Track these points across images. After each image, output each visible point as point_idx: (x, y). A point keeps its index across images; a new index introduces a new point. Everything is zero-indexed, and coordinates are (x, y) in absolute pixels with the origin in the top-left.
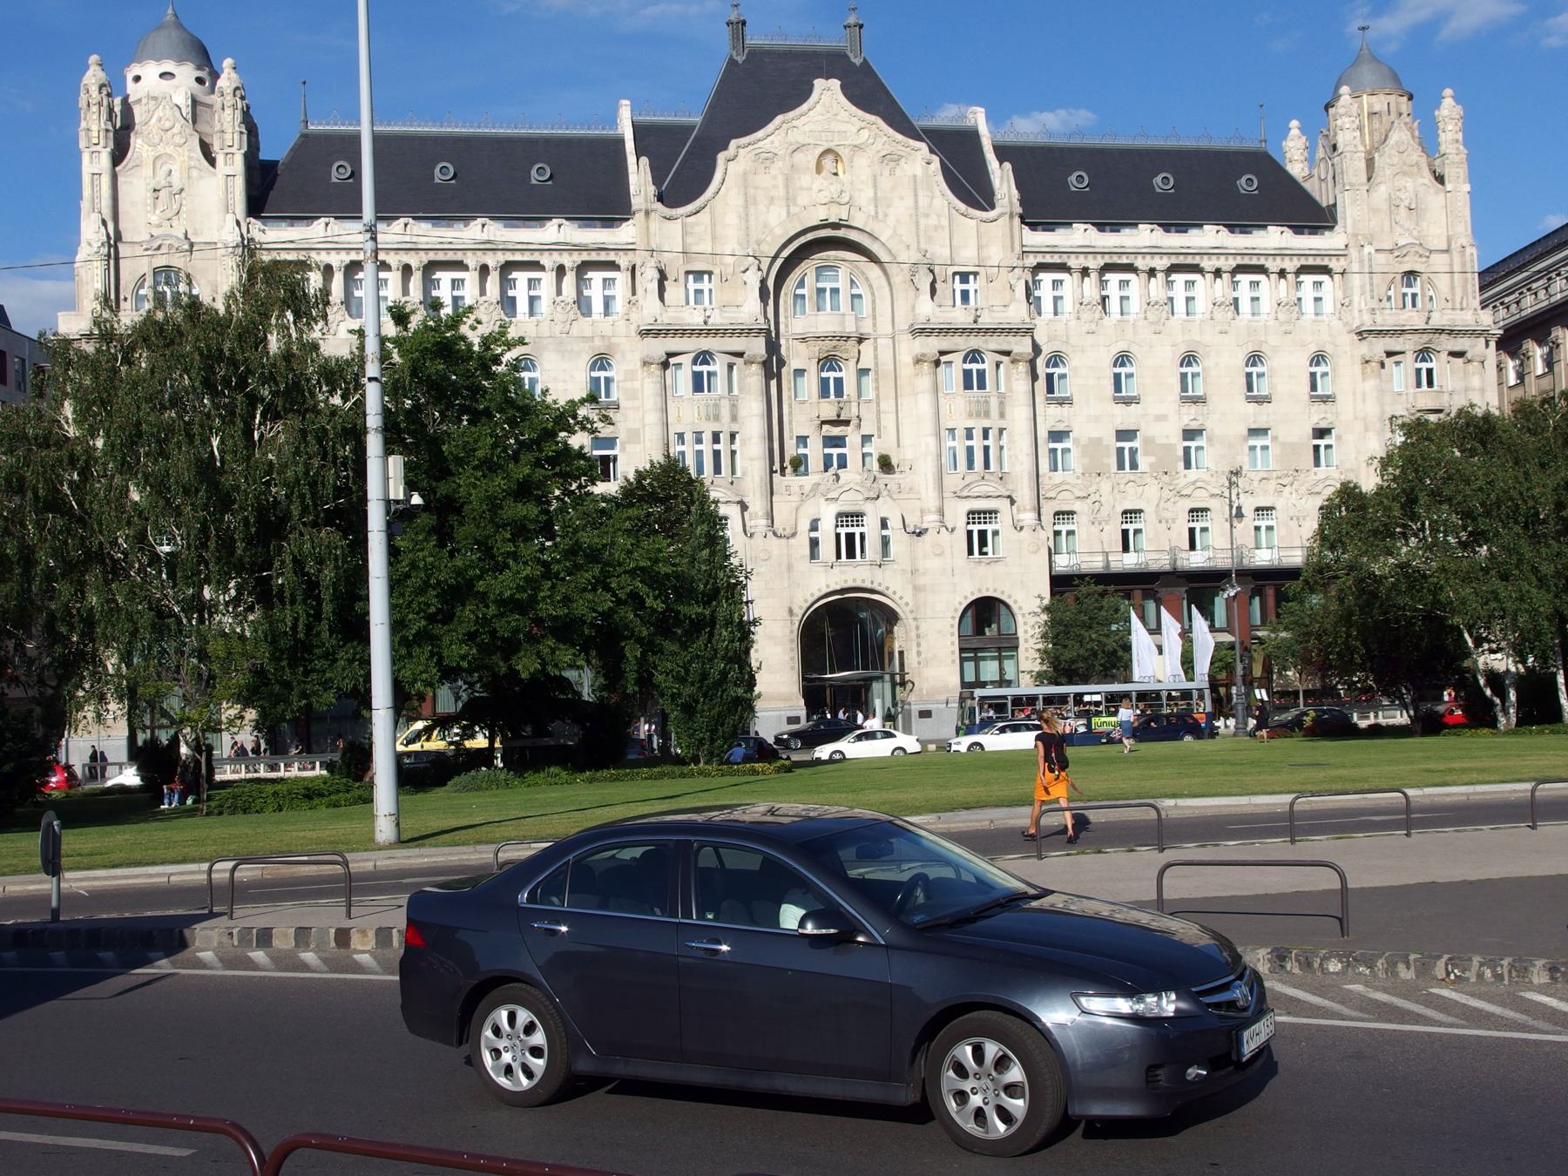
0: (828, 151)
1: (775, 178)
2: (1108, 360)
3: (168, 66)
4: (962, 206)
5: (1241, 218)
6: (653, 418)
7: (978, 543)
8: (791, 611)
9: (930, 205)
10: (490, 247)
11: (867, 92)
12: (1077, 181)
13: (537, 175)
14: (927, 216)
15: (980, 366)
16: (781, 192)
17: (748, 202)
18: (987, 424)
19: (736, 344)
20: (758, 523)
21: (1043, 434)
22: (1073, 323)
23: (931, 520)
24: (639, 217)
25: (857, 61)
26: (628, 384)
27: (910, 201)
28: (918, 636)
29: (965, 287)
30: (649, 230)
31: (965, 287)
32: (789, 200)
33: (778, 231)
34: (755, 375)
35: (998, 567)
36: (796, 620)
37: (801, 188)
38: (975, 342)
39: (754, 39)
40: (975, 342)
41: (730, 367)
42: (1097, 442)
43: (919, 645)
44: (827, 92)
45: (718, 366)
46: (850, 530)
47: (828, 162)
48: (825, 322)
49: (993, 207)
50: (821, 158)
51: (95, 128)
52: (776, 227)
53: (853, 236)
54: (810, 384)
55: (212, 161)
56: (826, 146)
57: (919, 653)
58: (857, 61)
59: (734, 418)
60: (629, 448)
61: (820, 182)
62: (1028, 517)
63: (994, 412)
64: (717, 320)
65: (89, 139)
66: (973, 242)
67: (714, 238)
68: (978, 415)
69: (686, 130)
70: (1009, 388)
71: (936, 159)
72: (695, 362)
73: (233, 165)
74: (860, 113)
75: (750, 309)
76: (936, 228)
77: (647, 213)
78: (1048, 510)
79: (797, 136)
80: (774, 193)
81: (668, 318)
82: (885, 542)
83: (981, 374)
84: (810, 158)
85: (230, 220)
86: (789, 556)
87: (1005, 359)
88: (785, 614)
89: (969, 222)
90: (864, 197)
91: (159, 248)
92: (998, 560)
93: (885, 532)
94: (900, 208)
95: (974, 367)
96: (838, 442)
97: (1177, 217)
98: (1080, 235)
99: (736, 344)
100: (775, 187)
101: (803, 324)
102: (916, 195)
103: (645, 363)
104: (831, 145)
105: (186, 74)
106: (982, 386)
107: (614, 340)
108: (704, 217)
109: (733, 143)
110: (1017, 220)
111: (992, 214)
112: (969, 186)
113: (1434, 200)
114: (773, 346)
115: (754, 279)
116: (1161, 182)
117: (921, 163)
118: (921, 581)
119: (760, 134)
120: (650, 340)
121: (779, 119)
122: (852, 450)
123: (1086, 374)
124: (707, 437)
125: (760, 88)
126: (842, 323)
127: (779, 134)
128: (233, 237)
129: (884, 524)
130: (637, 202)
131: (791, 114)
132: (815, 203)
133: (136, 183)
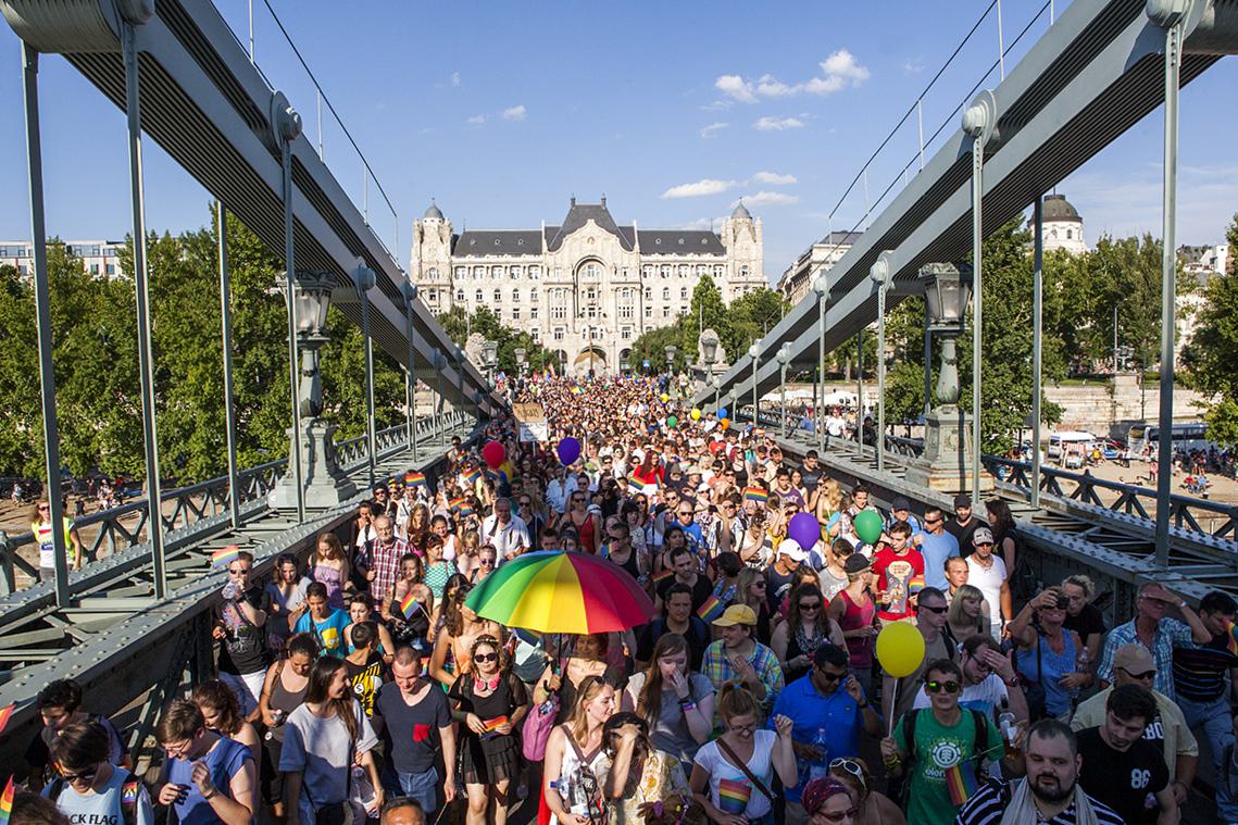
5: (699, 250)
6: (546, 304)
11: (605, 221)
17: (571, 250)
20: (570, 330)
21: (644, 308)
23: (614, 330)
30: (546, 258)
38: (626, 286)
40: (626, 286)
42: (658, 310)
44: (591, 222)
45: (562, 292)
48: (590, 279)
50: (590, 239)
52: (578, 257)
54: (586, 295)
62: (639, 329)
64: (561, 281)
69: (558, 228)
73: (448, 244)
75: (570, 278)
78: (644, 327)
79: (584, 234)
81: (550, 280)
89: (627, 254)
94: (609, 251)
97: (681, 251)
98: (656, 257)
101: (584, 279)
105: (437, 220)
112: (627, 245)
113: (753, 246)
114: (575, 286)
115: (571, 270)
116: (681, 241)
117: (614, 240)
122: (596, 311)
123: (657, 292)
125: (577, 218)
127: (577, 234)
128: (447, 261)
133: (425, 248)
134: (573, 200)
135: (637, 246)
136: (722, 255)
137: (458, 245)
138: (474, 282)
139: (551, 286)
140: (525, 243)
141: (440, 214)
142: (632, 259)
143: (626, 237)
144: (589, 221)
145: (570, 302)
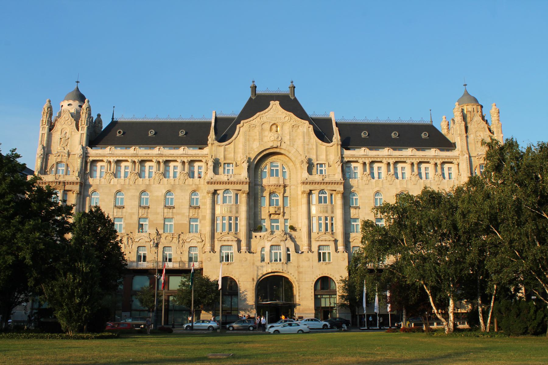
0: (274, 124)
1: (256, 133)
2: (372, 194)
3: (71, 102)
4: (321, 142)
6: (208, 212)
7: (321, 257)
8: (253, 279)
9: (309, 142)
10: (161, 155)
11: (291, 104)
12: (364, 135)
13: (182, 134)
14: (308, 145)
15: (325, 195)
16: (258, 137)
18: (326, 215)
19: (238, 187)
20: (244, 247)
22: (360, 181)
24: (210, 145)
25: (292, 98)
26: (203, 200)
27: (301, 140)
28: (299, 290)
29: (321, 169)
30: (213, 149)
31: (321, 169)
32: (261, 139)
33: (256, 150)
34: (243, 198)
35: (329, 266)
36: (255, 283)
37: (265, 136)
38: (322, 187)
39: (259, 91)
41: (237, 195)
43: (299, 293)
44: (275, 105)
45: (232, 194)
46: (276, 251)
47: (274, 127)
49: (332, 141)
50: (273, 127)
51: (45, 120)
53: (282, 152)
55: (78, 129)
56: (273, 122)
57: (299, 296)
58: (292, 98)
59: (237, 212)
60: (202, 222)
61: (271, 134)
62: (341, 248)
63: (329, 211)
64: (232, 179)
65: (42, 123)
66: (324, 154)
67: (235, 152)
68: (324, 212)
70: (335, 203)
71: (311, 126)
72: (224, 193)
73: (84, 130)
74: (286, 112)
75: (244, 175)
76: (311, 149)
77: (212, 144)
79: (264, 119)
80: (255, 138)
81: (217, 178)
82: (289, 255)
83: (325, 198)
84: (267, 126)
85: (80, 146)
86: (254, 260)
87: (334, 192)
88: (251, 280)
89: (323, 146)
90: (286, 138)
91: (59, 156)
92: (329, 263)
93: (289, 253)
94: (299, 142)
95: (323, 195)
96: (277, 221)
97: (397, 144)
99: (238, 187)
100: (256, 136)
102: (304, 138)
103: (208, 193)
104: (275, 122)
106: (325, 202)
107: (199, 186)
108: (232, 145)
109: (242, 122)
110: (339, 146)
111: (331, 144)
117: (306, 127)
118: (301, 270)
119: (251, 119)
120: (209, 185)
121: (258, 114)
124: (227, 218)
126: (279, 181)
129: (288, 250)
130: (210, 141)
131: (262, 112)
132: (269, 141)
134: (254, 88)
135: (337, 137)
136: (451, 150)
137: (97, 136)
138: (114, 181)
139: (216, 187)
140: (193, 134)
141: (81, 98)
142: (329, 153)
143: (322, 130)
144: (272, 103)
145: (243, 208)
